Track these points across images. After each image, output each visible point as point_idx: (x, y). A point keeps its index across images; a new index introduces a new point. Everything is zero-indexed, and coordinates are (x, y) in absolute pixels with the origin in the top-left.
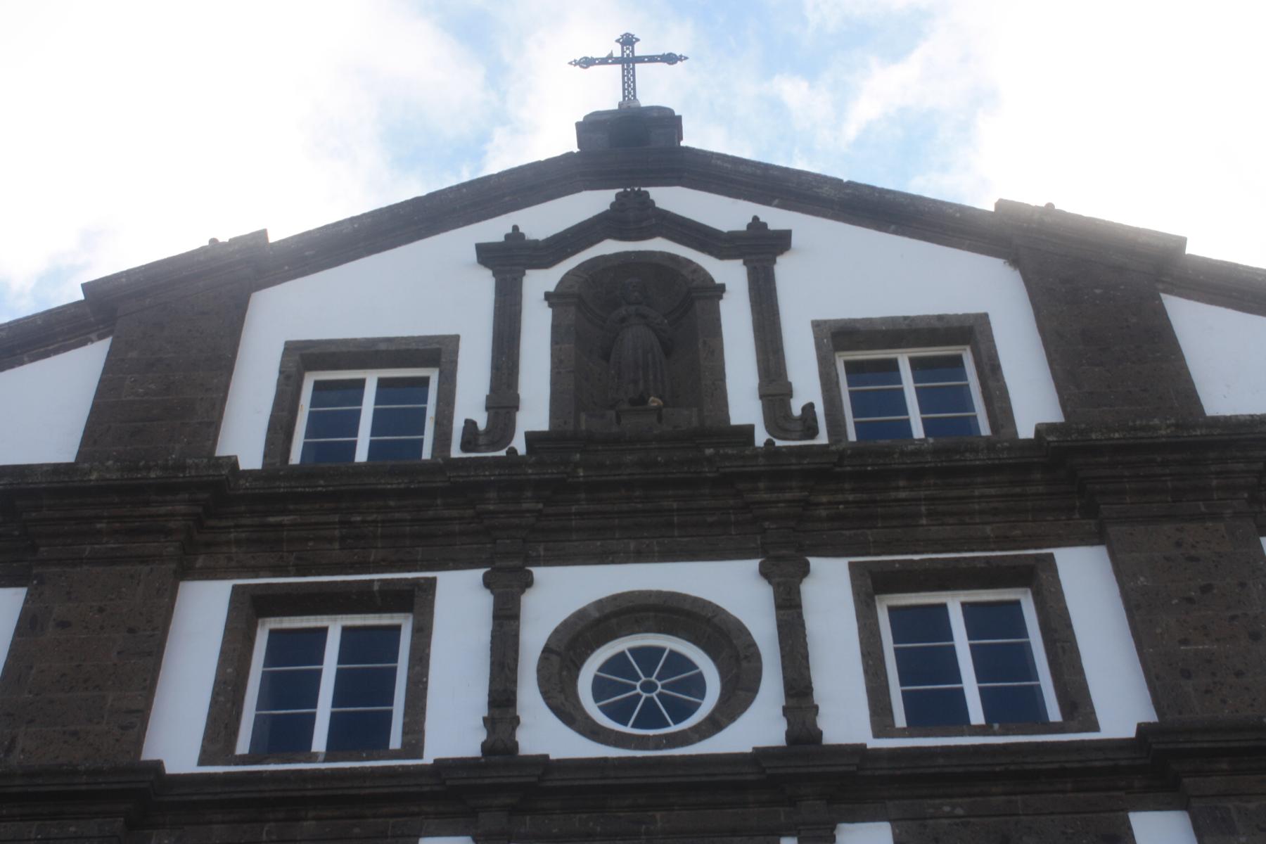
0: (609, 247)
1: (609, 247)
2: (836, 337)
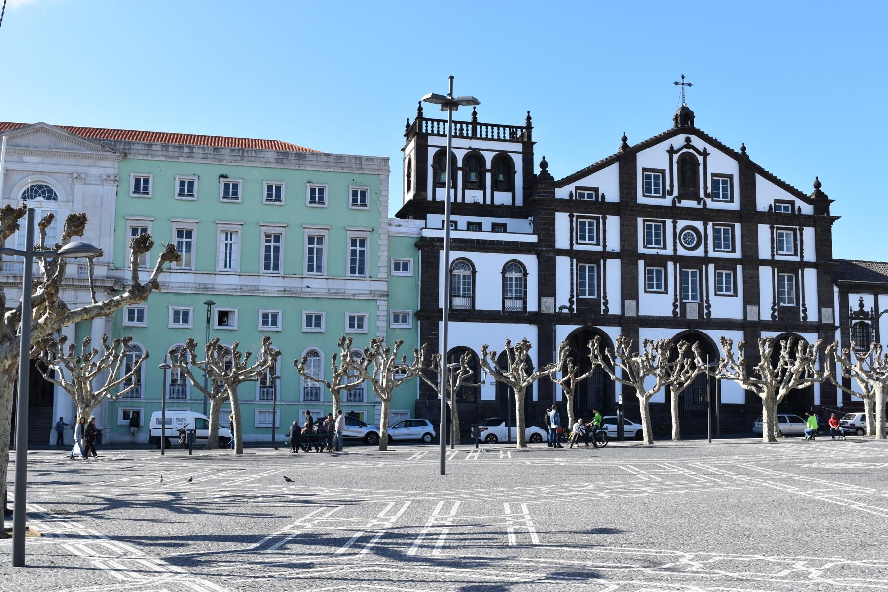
0: (685, 150)
1: (685, 150)
2: (713, 175)
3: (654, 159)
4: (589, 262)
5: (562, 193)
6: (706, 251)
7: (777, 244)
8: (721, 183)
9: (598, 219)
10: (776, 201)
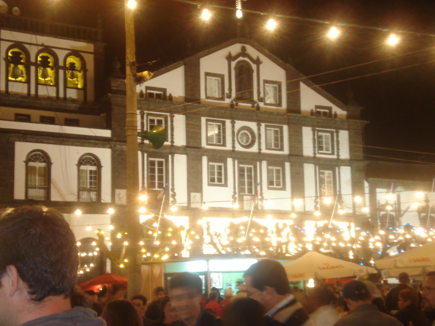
0: (241, 58)
1: (241, 58)
2: (266, 82)
6: (260, 149)
7: (318, 144)
9: (166, 118)
10: (317, 107)
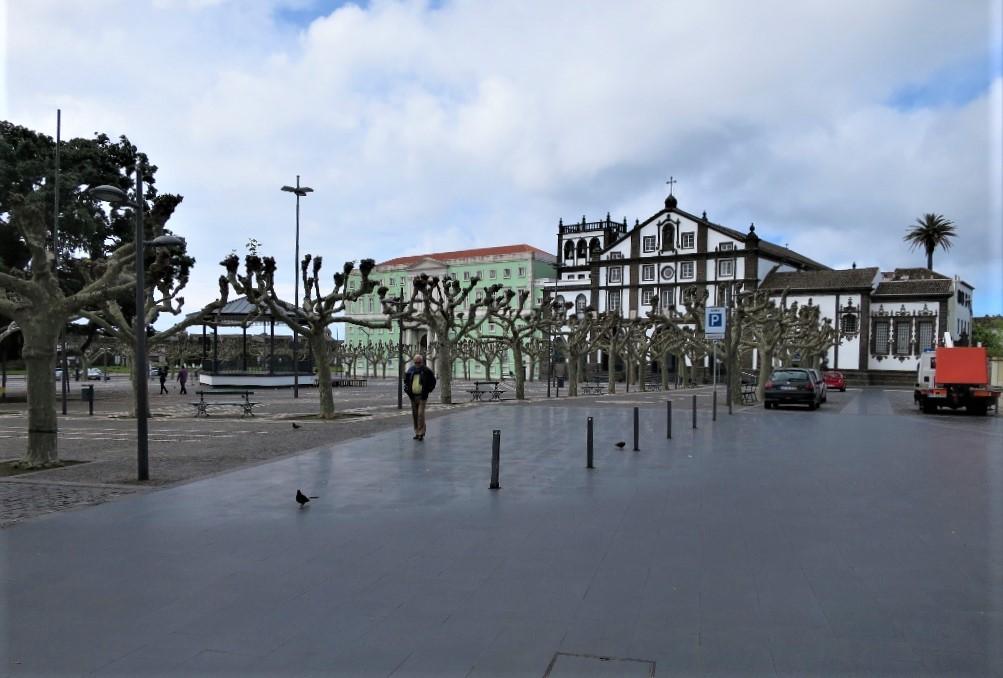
2: (683, 234)
3: (651, 230)
4: (614, 291)
5: (604, 257)
7: (718, 271)
8: (688, 237)
